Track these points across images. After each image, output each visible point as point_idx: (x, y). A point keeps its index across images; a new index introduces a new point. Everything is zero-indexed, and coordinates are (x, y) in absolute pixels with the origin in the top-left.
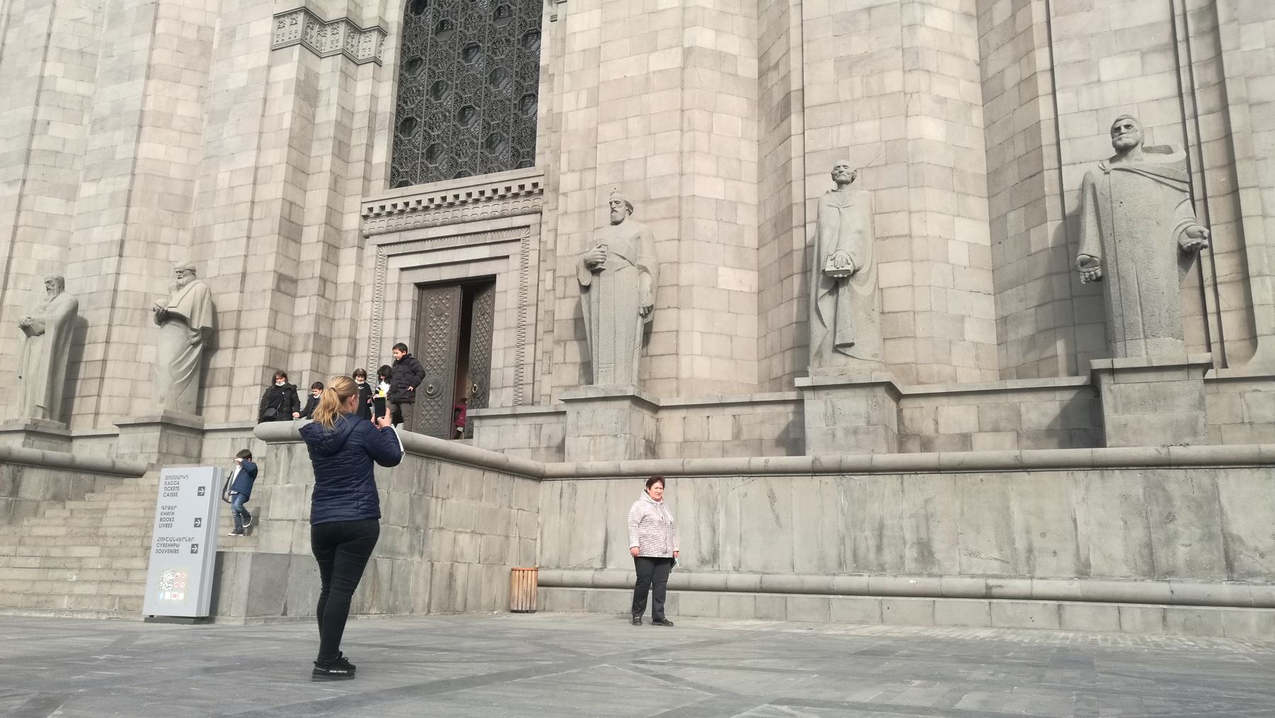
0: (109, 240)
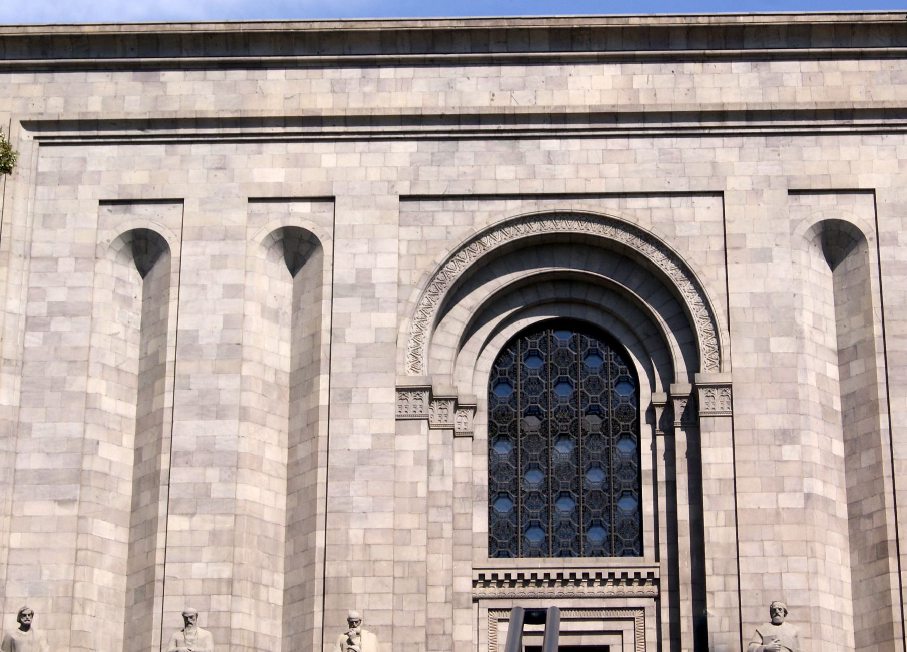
0: (216, 577)
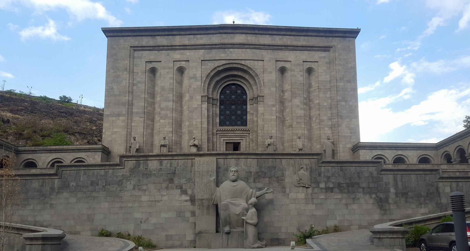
0: (169, 130)
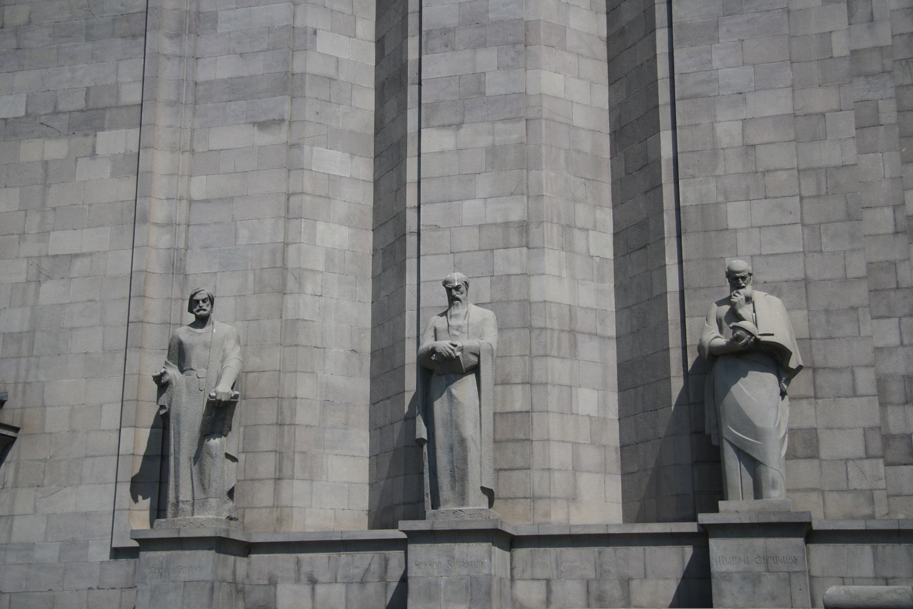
0: (499, 220)
